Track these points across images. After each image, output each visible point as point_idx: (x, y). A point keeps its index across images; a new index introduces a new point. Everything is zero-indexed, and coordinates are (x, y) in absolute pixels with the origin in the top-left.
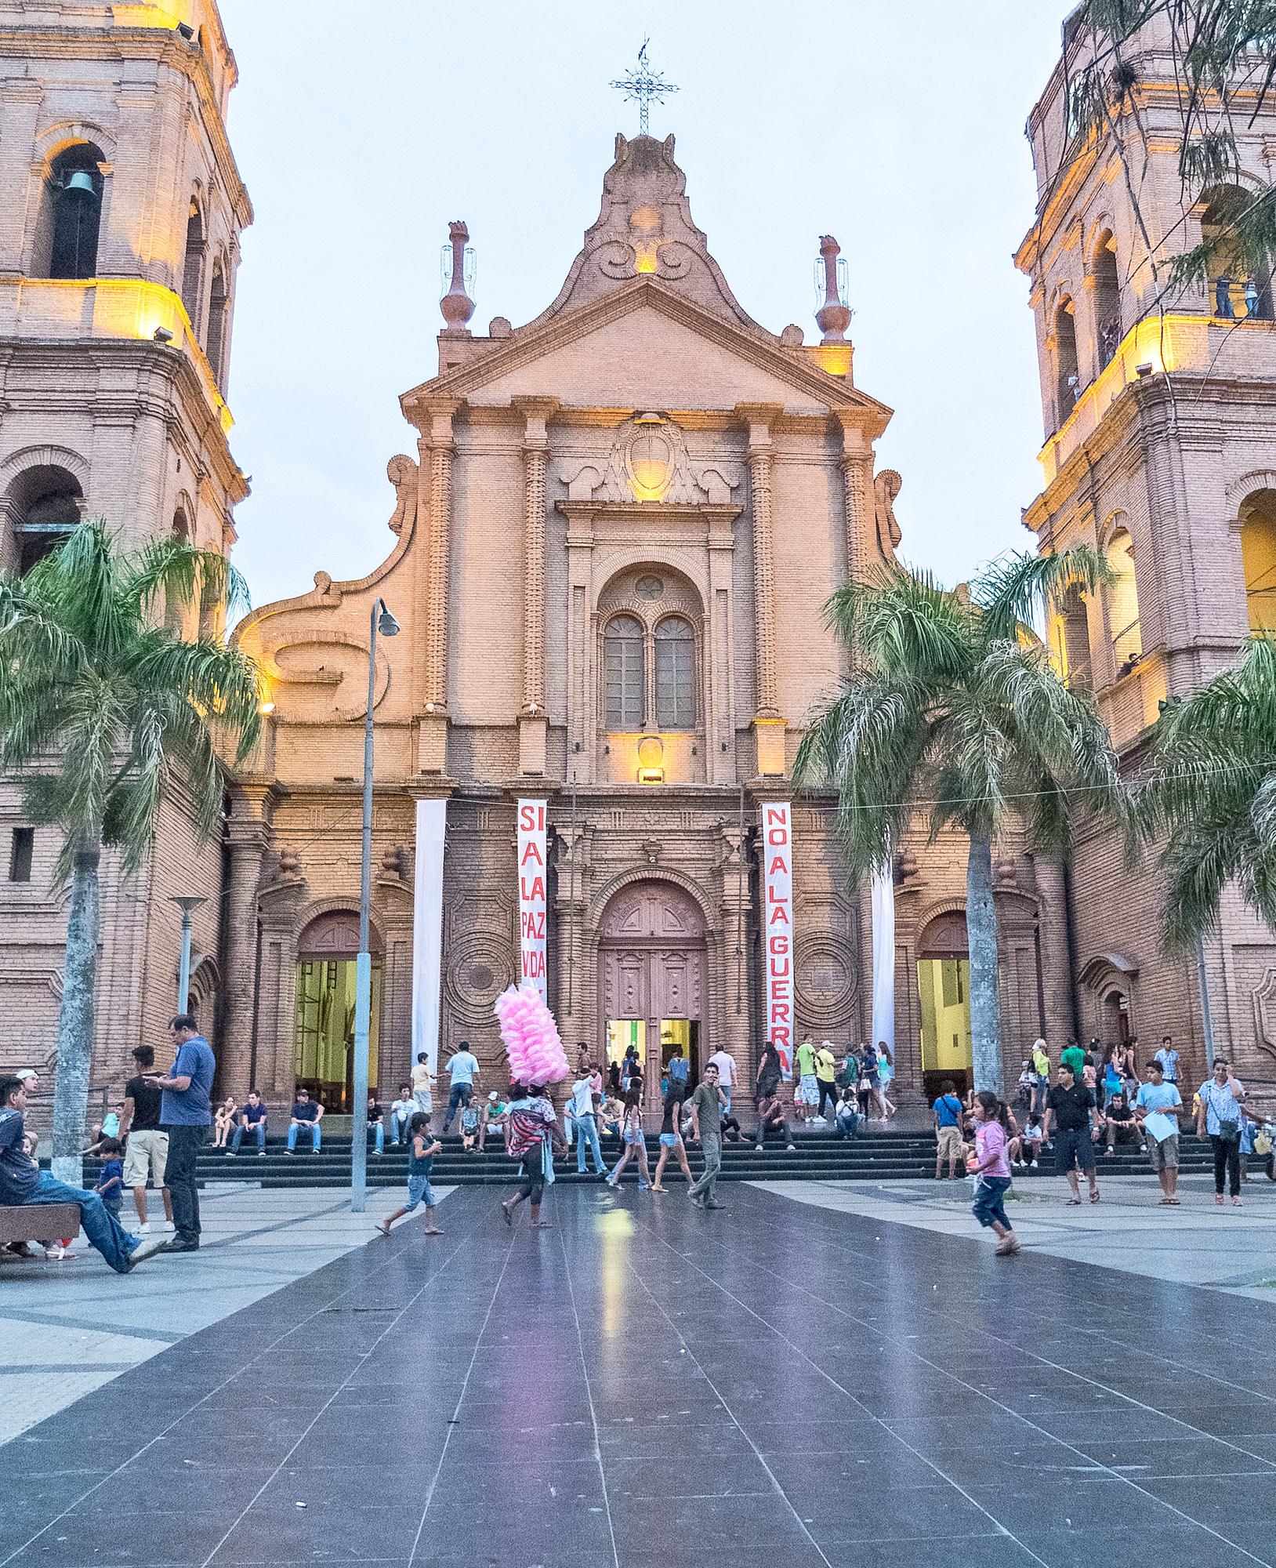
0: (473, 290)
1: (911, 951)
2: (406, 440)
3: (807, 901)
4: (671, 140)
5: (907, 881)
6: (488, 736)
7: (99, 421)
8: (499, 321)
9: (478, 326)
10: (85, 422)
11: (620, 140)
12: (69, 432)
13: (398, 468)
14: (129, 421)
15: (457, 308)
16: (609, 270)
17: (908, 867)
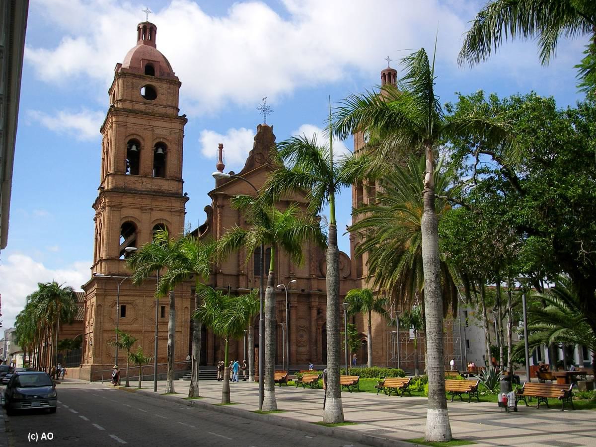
0: (226, 162)
1: (321, 329)
2: (209, 202)
3: (299, 318)
4: (272, 126)
5: (321, 315)
6: (230, 277)
7: (173, 214)
8: (232, 173)
9: (226, 173)
10: (169, 213)
11: (260, 125)
12: (166, 216)
13: (208, 209)
14: (178, 214)
15: (221, 168)
16: (257, 160)
17: (321, 311)
